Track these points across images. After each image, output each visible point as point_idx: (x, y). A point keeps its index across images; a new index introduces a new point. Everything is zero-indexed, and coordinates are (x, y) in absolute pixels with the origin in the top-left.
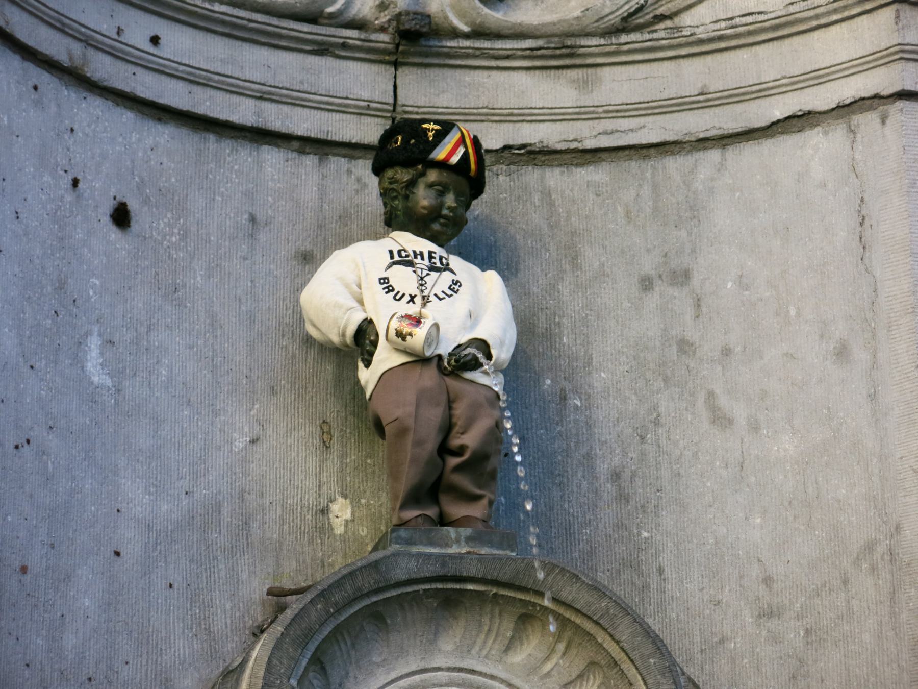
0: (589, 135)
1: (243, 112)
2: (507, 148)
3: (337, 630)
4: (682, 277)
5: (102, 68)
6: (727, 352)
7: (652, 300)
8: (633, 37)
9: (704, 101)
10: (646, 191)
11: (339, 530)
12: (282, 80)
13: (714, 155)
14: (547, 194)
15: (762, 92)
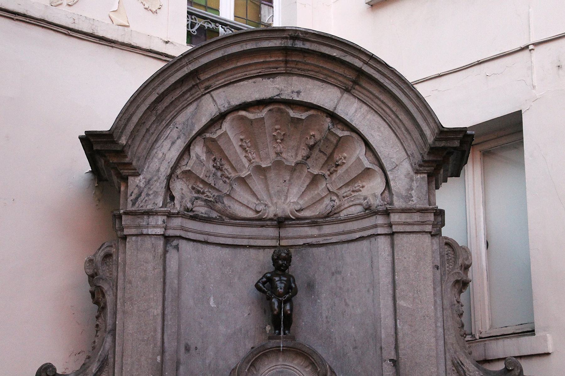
0: (321, 240)
1: (245, 242)
2: (304, 244)
3: (256, 360)
4: (339, 272)
5: (212, 239)
6: (348, 290)
7: (334, 278)
8: (329, 219)
9: (344, 233)
10: (333, 253)
11: (268, 332)
12: (254, 234)
13: (346, 245)
14: (313, 254)
15: (354, 231)
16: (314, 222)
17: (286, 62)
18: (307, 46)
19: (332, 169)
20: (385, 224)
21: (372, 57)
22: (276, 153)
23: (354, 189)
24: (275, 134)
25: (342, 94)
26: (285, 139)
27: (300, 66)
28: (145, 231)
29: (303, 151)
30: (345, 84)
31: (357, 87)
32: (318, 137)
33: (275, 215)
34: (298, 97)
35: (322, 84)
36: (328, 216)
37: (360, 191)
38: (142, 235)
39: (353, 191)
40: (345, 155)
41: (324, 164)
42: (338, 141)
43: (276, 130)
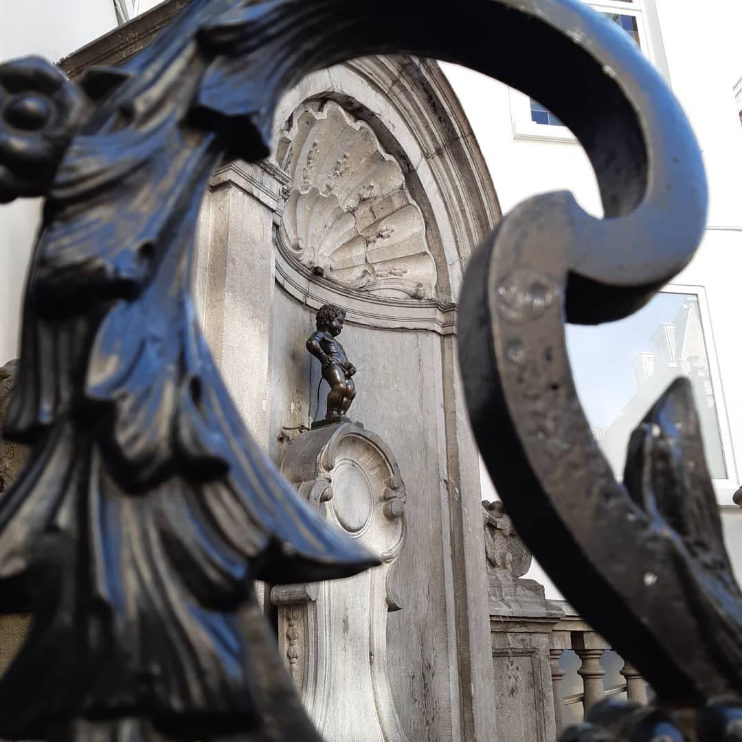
13: (377, 332)
15: (393, 319)
16: (347, 291)
17: (396, 81)
18: (428, 77)
19: (372, 238)
20: (440, 322)
21: (472, 133)
22: (327, 186)
23: (393, 271)
24: (339, 160)
25: (422, 157)
26: (344, 175)
27: (402, 97)
28: (256, 192)
29: (352, 200)
30: (428, 145)
31: (437, 157)
32: (375, 192)
33: (311, 263)
34: (393, 130)
35: (409, 133)
36: (359, 290)
37: (402, 276)
38: (250, 194)
39: (391, 273)
40: (393, 226)
41: (367, 228)
42: (402, 208)
43: (345, 157)
